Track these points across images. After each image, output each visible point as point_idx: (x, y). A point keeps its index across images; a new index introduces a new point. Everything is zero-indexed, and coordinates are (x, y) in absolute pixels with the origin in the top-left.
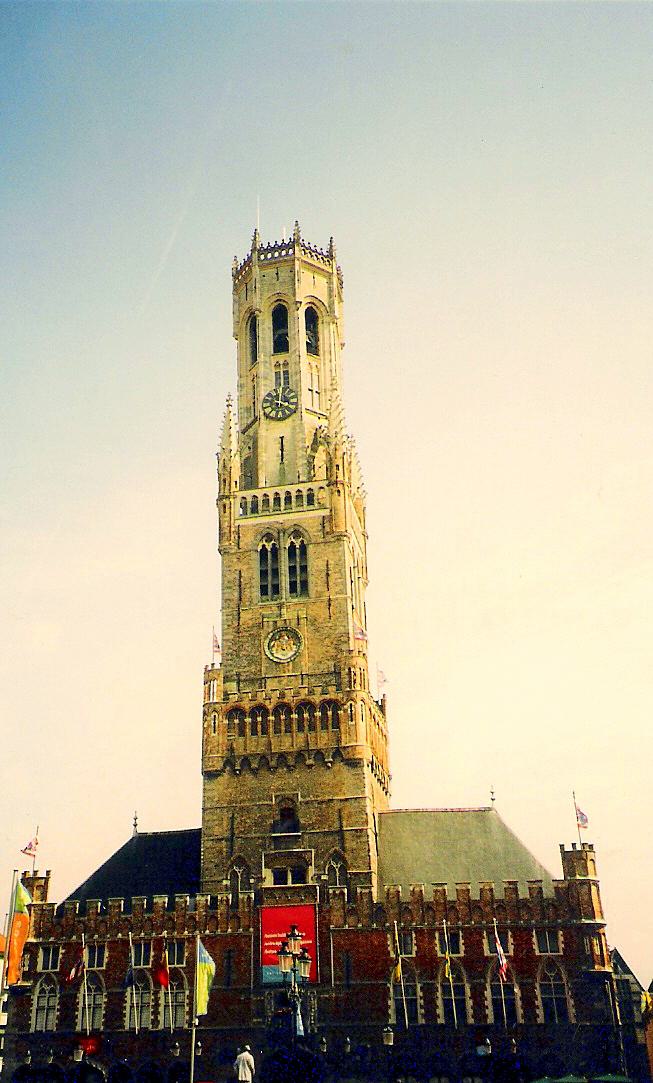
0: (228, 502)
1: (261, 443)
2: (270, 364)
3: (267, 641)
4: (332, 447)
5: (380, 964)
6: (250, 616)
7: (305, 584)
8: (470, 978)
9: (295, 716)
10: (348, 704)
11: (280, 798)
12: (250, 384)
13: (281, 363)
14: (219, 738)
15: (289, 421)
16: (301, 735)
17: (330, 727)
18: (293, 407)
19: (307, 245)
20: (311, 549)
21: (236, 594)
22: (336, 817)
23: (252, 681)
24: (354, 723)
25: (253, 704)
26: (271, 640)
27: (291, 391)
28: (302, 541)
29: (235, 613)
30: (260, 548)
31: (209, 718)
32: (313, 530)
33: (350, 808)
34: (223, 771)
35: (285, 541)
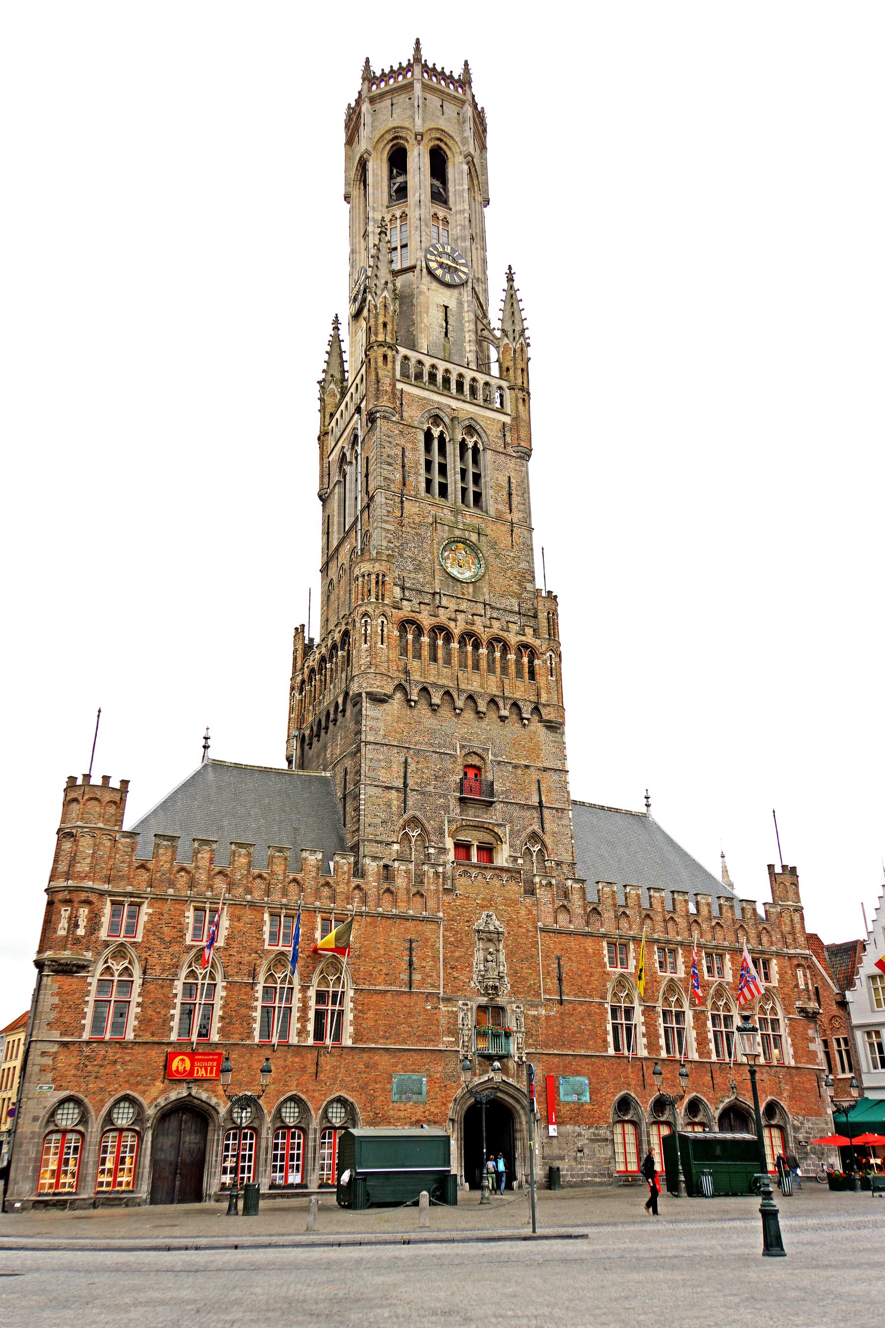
0: (390, 353)
4: (518, 346)
5: (596, 978)
7: (477, 496)
9: (483, 651)
10: (548, 654)
11: (467, 751)
13: (441, 215)
15: (456, 292)
16: (492, 678)
17: (526, 675)
18: (464, 277)
21: (398, 476)
22: (534, 787)
24: (554, 679)
25: (434, 621)
28: (476, 443)
29: (398, 500)
30: (425, 427)
31: (374, 622)
32: (493, 434)
34: (390, 697)
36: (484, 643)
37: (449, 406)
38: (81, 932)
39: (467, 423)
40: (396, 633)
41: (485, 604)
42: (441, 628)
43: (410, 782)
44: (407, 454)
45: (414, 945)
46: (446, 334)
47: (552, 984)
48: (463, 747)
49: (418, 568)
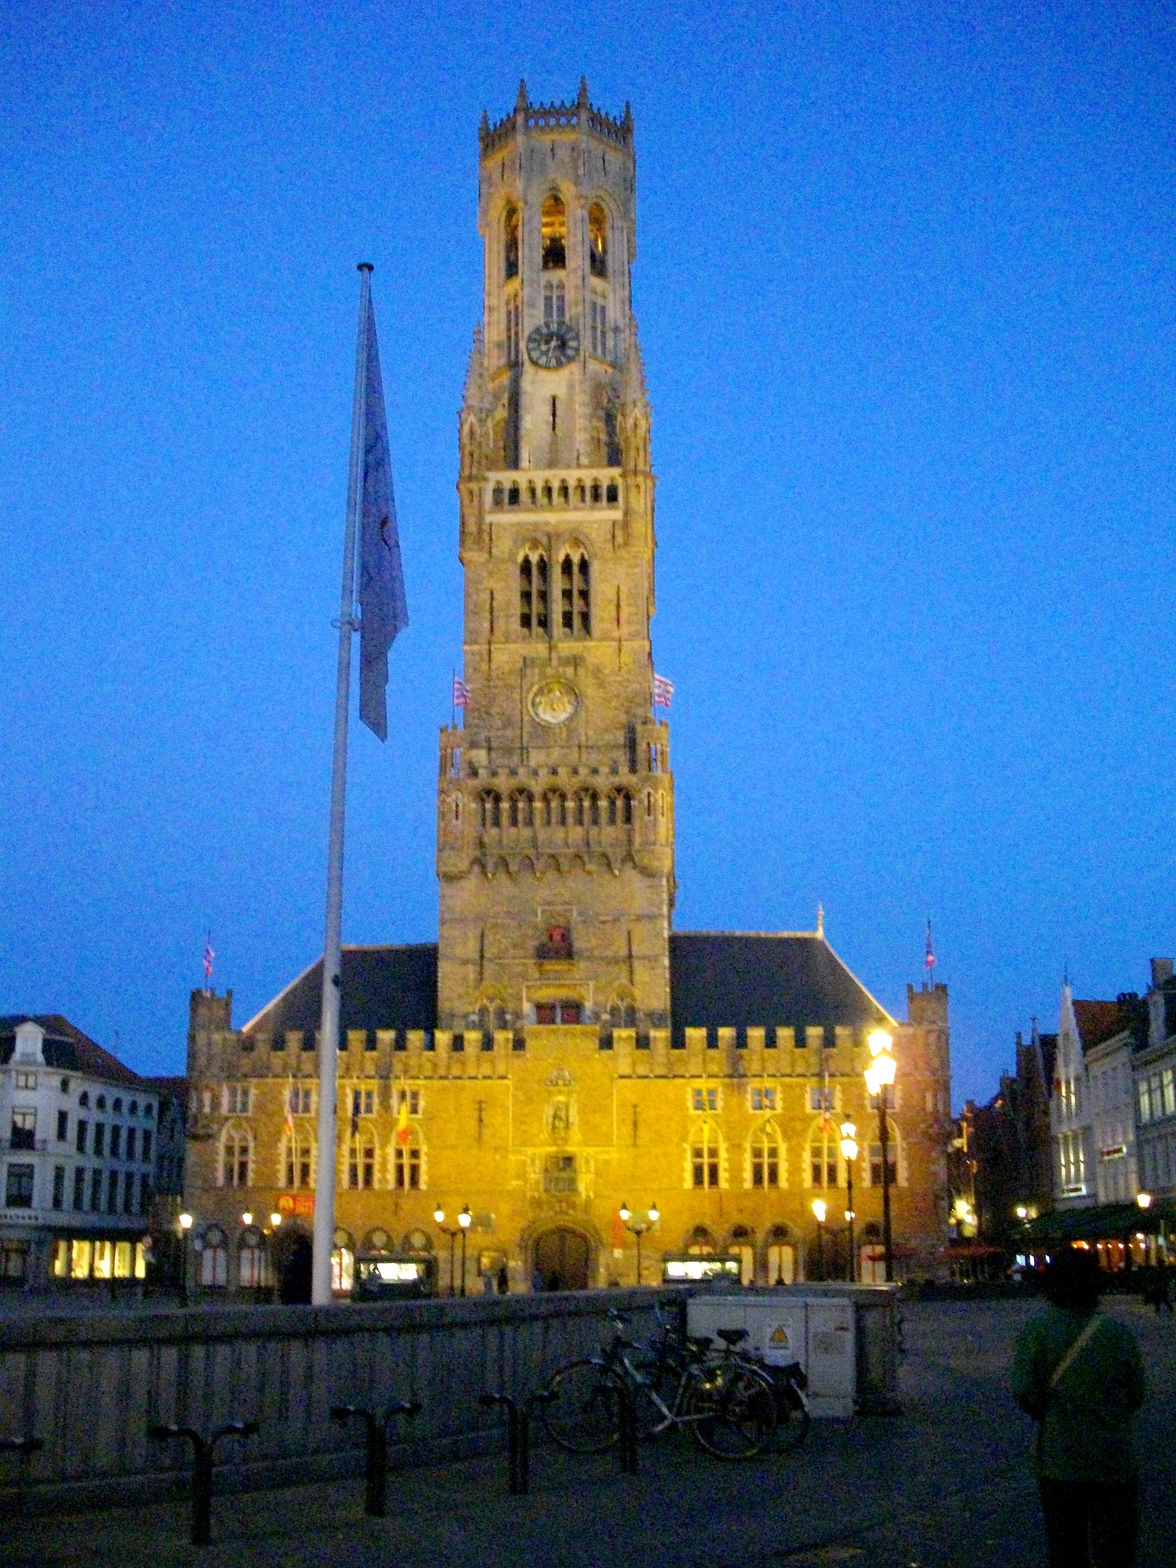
1: (525, 401)
2: (539, 285)
3: (531, 696)
6: (505, 658)
7: (585, 617)
8: (787, 1136)
10: (646, 792)
12: (503, 310)
13: (555, 283)
14: (466, 827)
15: (565, 373)
19: (596, 111)
20: (595, 568)
21: (487, 625)
23: (508, 751)
24: (652, 817)
25: (514, 782)
26: (536, 695)
27: (570, 329)
29: (485, 652)
30: (520, 558)
33: (641, 932)
34: (469, 872)
35: (558, 549)
36: (569, 796)
37: (547, 523)
38: (207, 1110)
39: (567, 537)
40: (473, 805)
41: (580, 747)
42: (521, 791)
43: (487, 955)
44: (496, 595)
45: (484, 1106)
46: (554, 428)
47: (627, 1129)
48: (543, 912)
49: (507, 724)
